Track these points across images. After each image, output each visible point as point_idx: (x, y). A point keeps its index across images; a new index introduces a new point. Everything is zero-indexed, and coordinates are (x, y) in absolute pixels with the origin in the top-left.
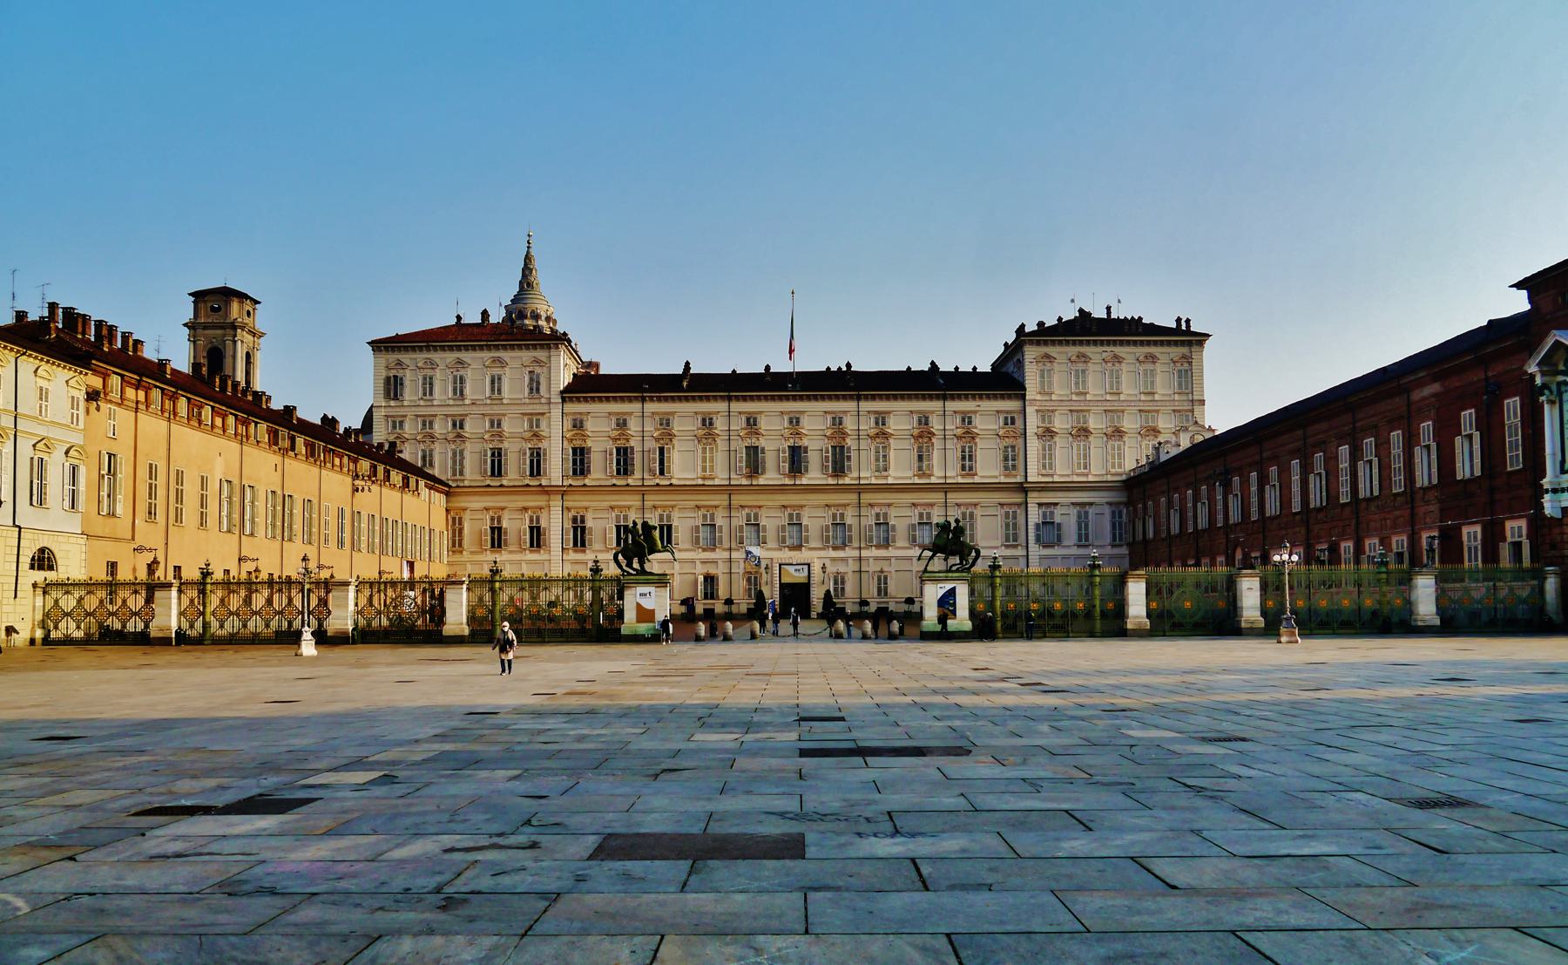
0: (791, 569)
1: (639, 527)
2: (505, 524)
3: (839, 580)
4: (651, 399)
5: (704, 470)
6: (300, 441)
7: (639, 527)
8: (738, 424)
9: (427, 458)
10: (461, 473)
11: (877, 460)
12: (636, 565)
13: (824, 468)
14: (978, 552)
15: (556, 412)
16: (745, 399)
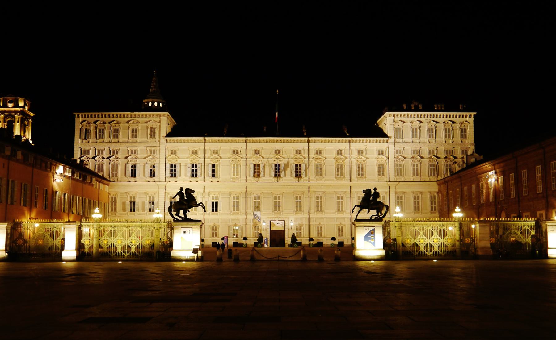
0: (276, 223)
1: (184, 191)
2: (137, 201)
3: (299, 228)
4: (209, 141)
5: (234, 175)
6: (19, 155)
7: (184, 191)
8: (251, 153)
9: (100, 168)
10: (116, 176)
11: (317, 171)
12: (181, 213)
13: (291, 175)
14: (388, 208)
15: (163, 146)
16: (253, 141)
